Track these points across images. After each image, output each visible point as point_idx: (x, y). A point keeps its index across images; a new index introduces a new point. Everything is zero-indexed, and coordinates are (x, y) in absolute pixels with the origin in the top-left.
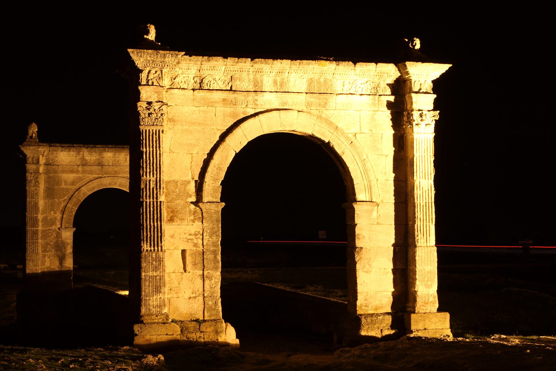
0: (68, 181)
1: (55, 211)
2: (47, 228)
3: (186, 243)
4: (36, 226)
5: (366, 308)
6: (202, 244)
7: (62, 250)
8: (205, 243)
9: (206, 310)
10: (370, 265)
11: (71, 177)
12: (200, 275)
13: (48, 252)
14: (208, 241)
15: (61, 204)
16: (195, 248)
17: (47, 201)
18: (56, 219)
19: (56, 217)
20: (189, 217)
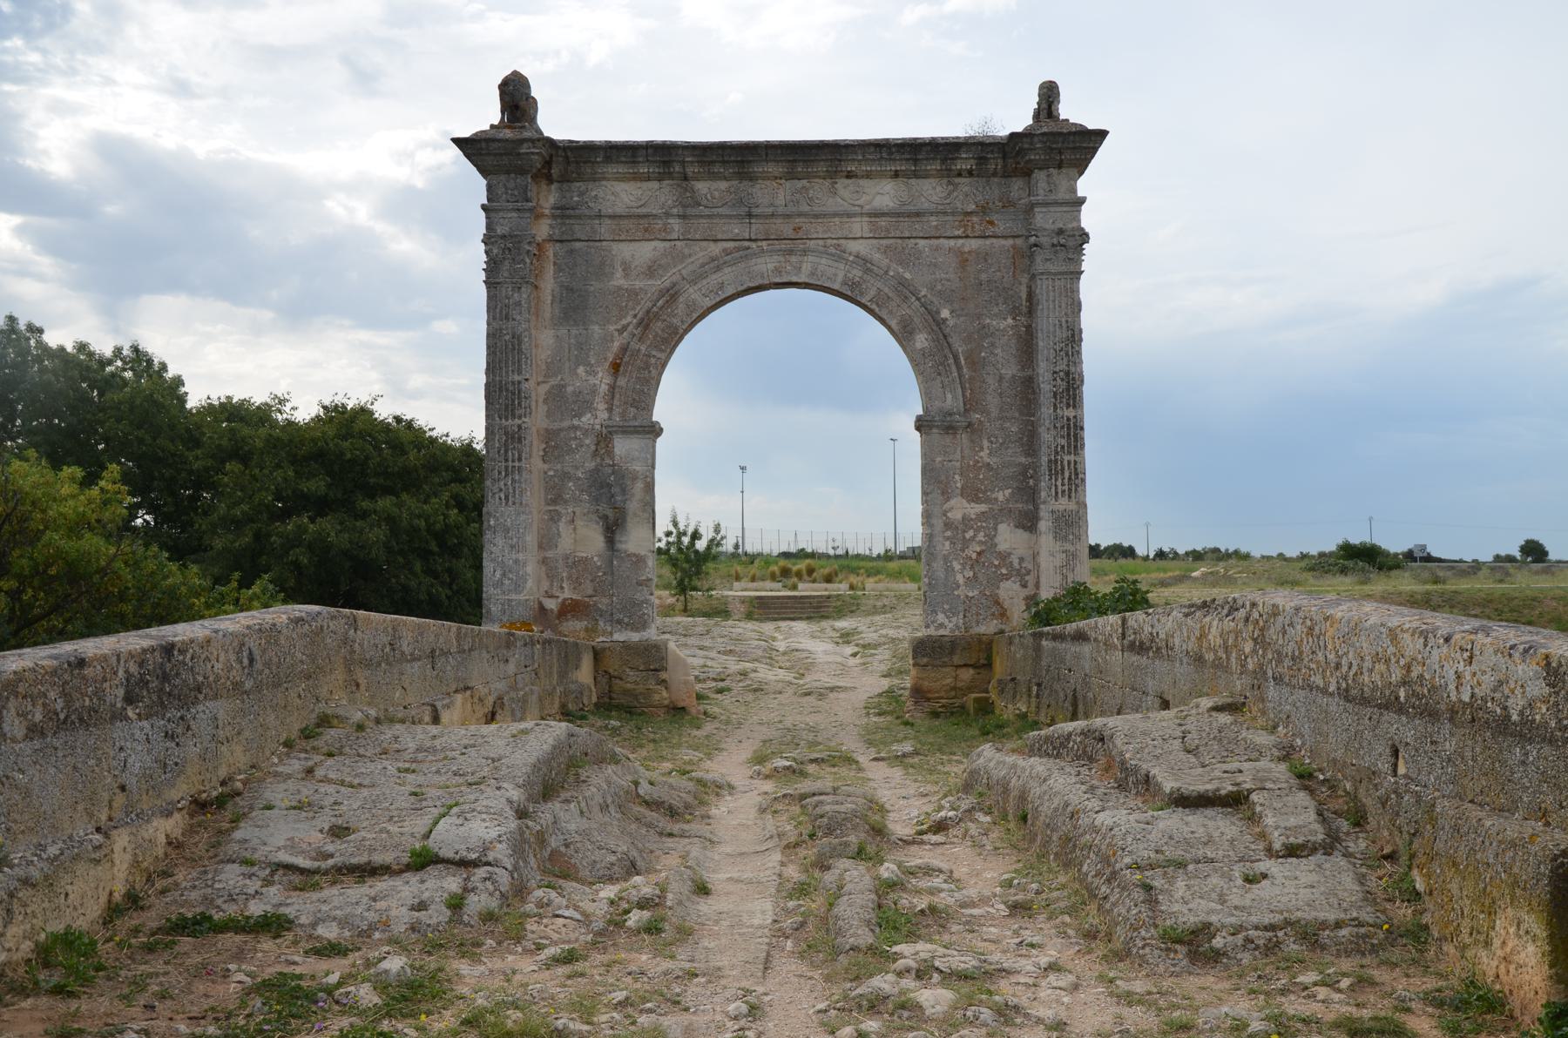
0: (637, 263)
1: (589, 364)
2: (566, 424)
7: (613, 496)
11: (644, 252)
13: (566, 502)
15: (613, 341)
17: (563, 331)
18: (594, 391)
19: (595, 385)
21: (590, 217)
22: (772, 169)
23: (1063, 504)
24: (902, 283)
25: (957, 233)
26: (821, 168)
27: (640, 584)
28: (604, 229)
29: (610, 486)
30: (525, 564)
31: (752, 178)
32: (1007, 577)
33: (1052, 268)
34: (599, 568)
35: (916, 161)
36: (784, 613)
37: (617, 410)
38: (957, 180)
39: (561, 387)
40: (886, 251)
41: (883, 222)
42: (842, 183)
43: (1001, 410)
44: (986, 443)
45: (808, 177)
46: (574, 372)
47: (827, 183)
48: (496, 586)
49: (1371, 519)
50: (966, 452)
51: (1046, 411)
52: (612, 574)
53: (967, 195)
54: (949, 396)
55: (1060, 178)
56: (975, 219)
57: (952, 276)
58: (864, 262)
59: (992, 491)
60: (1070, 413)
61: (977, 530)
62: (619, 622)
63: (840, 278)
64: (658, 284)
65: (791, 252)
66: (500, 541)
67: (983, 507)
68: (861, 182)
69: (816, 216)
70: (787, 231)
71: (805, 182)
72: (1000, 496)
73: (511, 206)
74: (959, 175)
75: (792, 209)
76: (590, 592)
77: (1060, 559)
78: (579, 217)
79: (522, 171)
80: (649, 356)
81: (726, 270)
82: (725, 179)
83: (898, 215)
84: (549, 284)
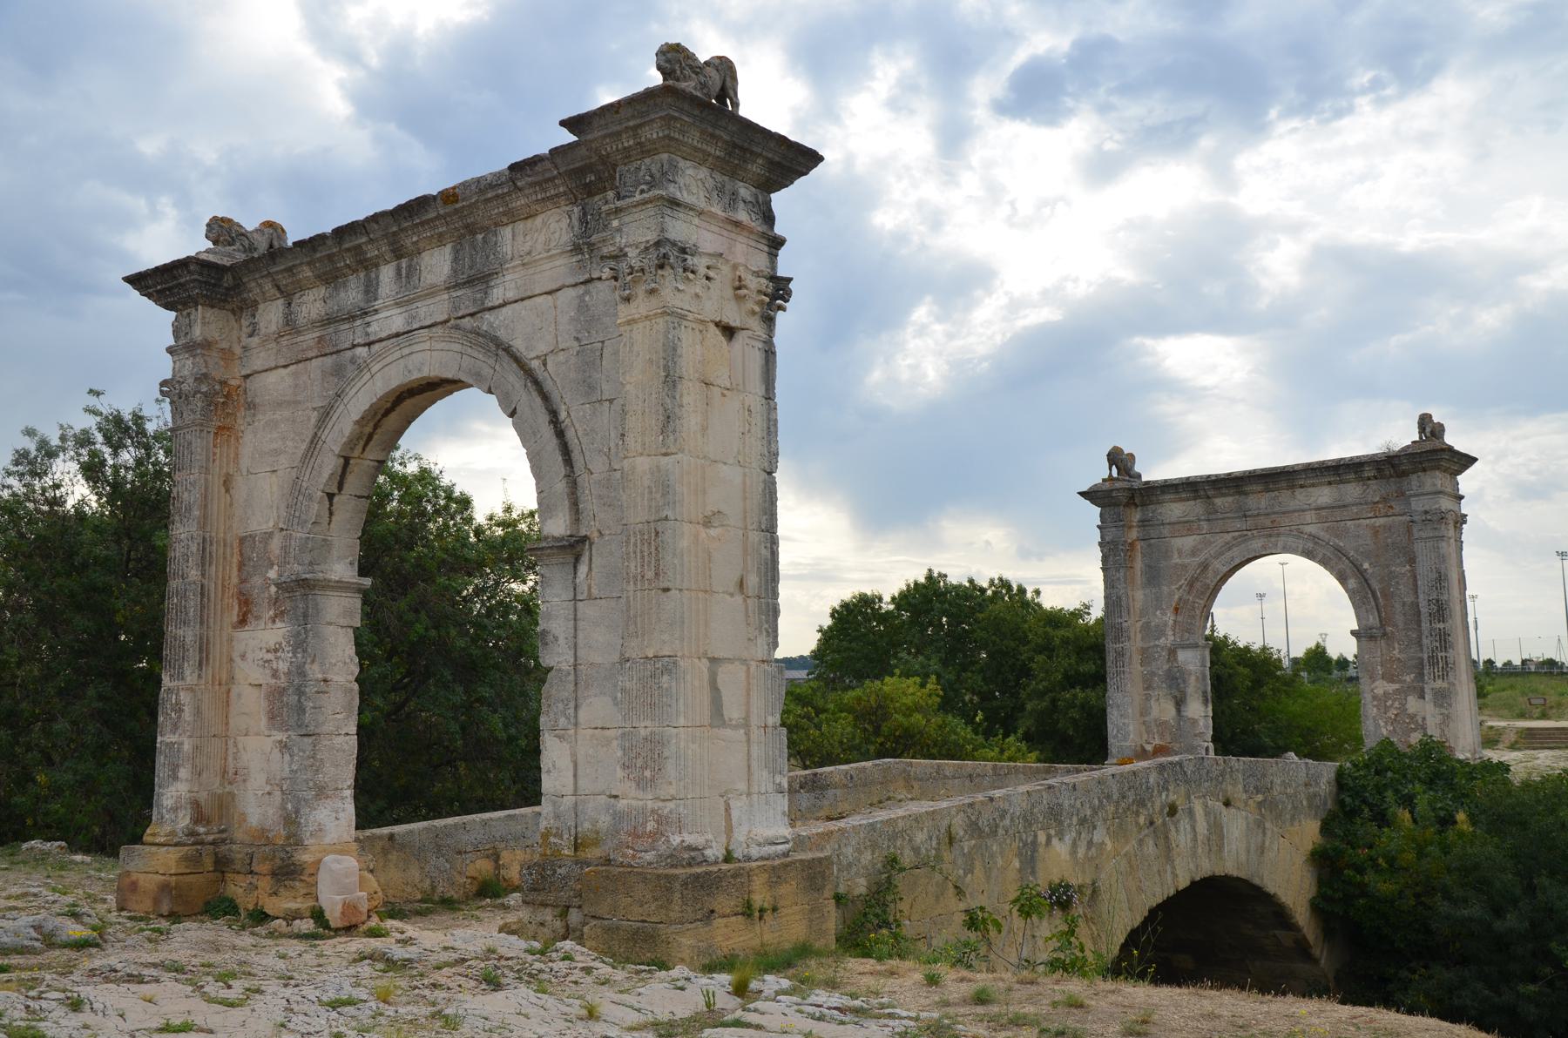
2: (1152, 644)
3: (261, 670)
11: (1188, 542)
14: (291, 662)
17: (1148, 591)
18: (1166, 625)
23: (1439, 684)
24: (1338, 549)
25: (1370, 515)
26: (1284, 484)
27: (1196, 735)
29: (1177, 679)
31: (1246, 494)
32: (1414, 730)
33: (1423, 535)
35: (1339, 475)
36: (1547, 743)
38: (1369, 482)
39: (1148, 623)
41: (1324, 513)
42: (1298, 491)
43: (1405, 624)
44: (1396, 646)
45: (1278, 490)
47: (1289, 492)
50: (1384, 651)
51: (1425, 625)
53: (1375, 490)
54: (1371, 617)
56: (1380, 506)
57: (1369, 542)
58: (1313, 537)
59: (1402, 675)
61: (1395, 700)
64: (1197, 560)
65: (1270, 536)
67: (1397, 686)
68: (1310, 489)
69: (1284, 513)
72: (1408, 678)
73: (1111, 525)
74: (1369, 479)
75: (1266, 511)
76: (1169, 740)
77: (1439, 719)
79: (1116, 505)
81: (1235, 549)
83: (1333, 507)
84: (1139, 564)
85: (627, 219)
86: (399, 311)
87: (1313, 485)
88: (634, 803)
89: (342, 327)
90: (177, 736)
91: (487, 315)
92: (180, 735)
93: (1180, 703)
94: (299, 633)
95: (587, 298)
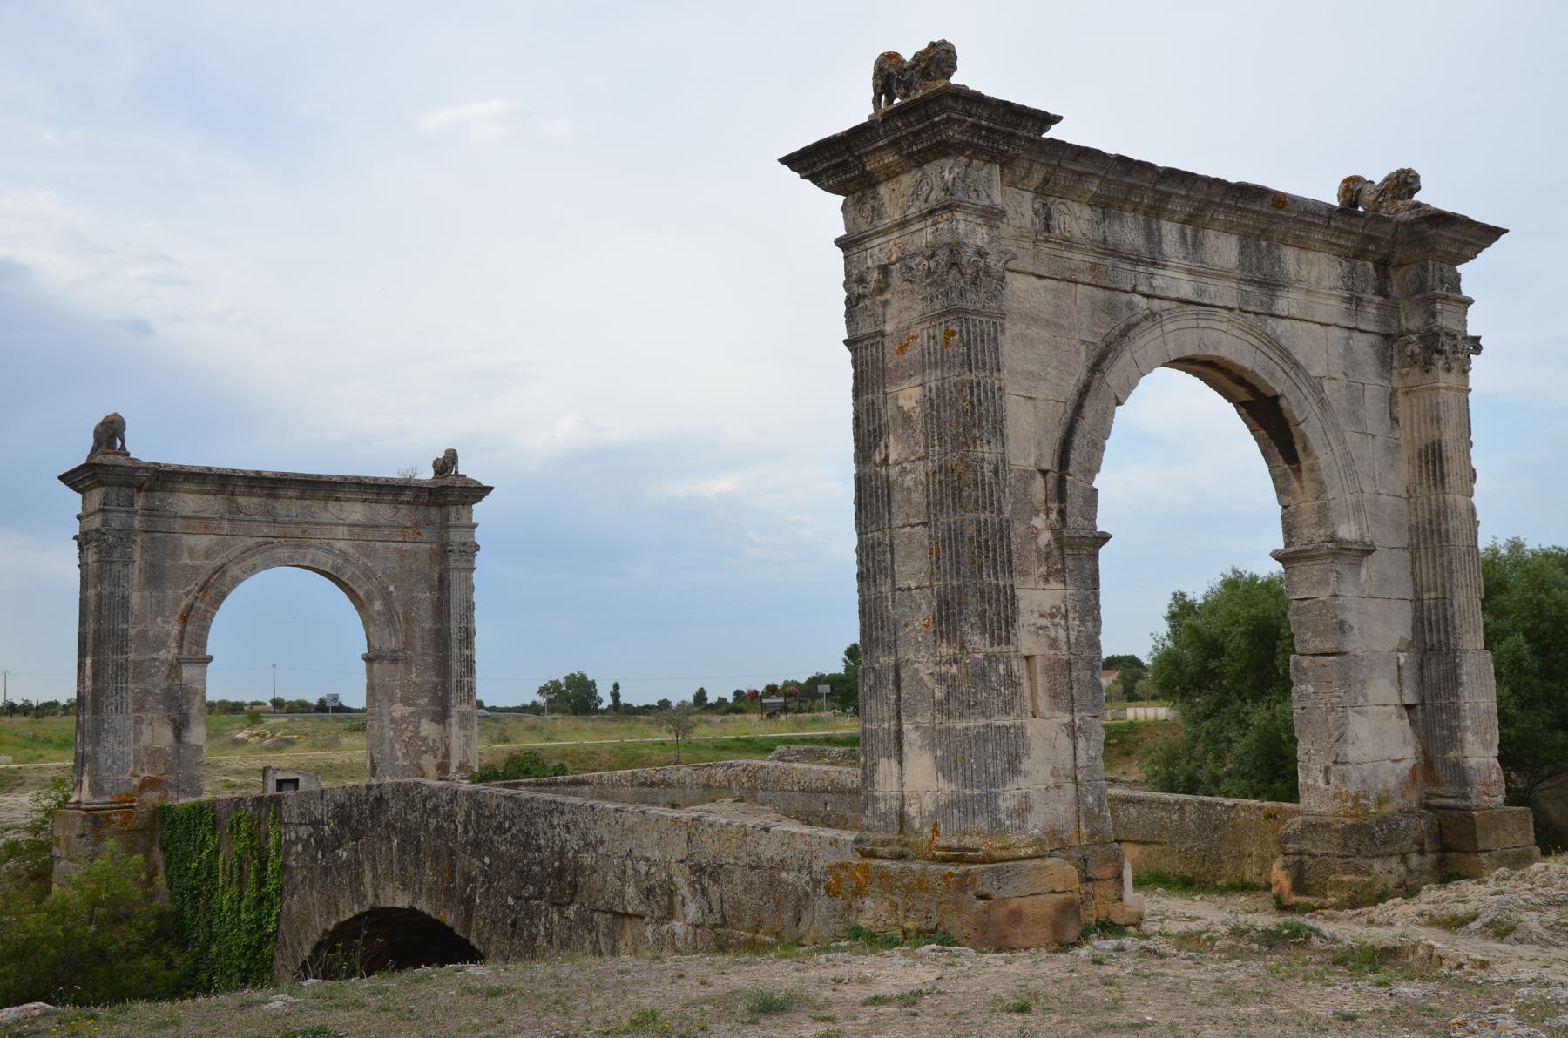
0: (198, 549)
2: (148, 657)
4: (125, 650)
5: (1365, 802)
6: (1065, 640)
8: (1072, 640)
9: (1083, 819)
10: (1365, 696)
11: (203, 541)
12: (1065, 724)
13: (147, 710)
14: (1079, 632)
16: (1052, 652)
17: (147, 593)
18: (168, 634)
20: (1038, 568)
21: (169, 517)
22: (290, 493)
24: (368, 568)
26: (322, 494)
27: (198, 765)
28: (178, 525)
29: (178, 699)
30: (129, 755)
31: (275, 497)
32: (425, 752)
33: (459, 565)
34: (169, 755)
37: (186, 648)
39: (145, 632)
40: (357, 548)
41: (356, 530)
42: (331, 503)
43: (423, 648)
44: (414, 669)
45: (311, 498)
46: (154, 621)
48: (110, 769)
49: (274, 666)
51: (455, 651)
52: (179, 759)
53: (405, 515)
54: (393, 640)
55: (464, 512)
57: (395, 565)
58: (345, 555)
60: (468, 652)
61: (409, 724)
62: (183, 791)
63: (329, 565)
65: (300, 546)
66: (111, 738)
67: (411, 709)
68: (344, 504)
69: (316, 524)
70: (298, 532)
71: (308, 502)
72: (422, 702)
73: (123, 509)
74: (402, 503)
75: (299, 520)
76: (163, 771)
77: (462, 741)
78: (160, 516)
80: (207, 611)
81: (258, 556)
82: (259, 496)
83: (366, 526)
85: (1446, 307)
86: (1186, 277)
87: (348, 500)
88: (1481, 760)
89: (1122, 265)
90: (1012, 716)
91: (1270, 320)
92: (1018, 716)
93: (180, 728)
94: (1087, 599)
95: (1351, 342)
